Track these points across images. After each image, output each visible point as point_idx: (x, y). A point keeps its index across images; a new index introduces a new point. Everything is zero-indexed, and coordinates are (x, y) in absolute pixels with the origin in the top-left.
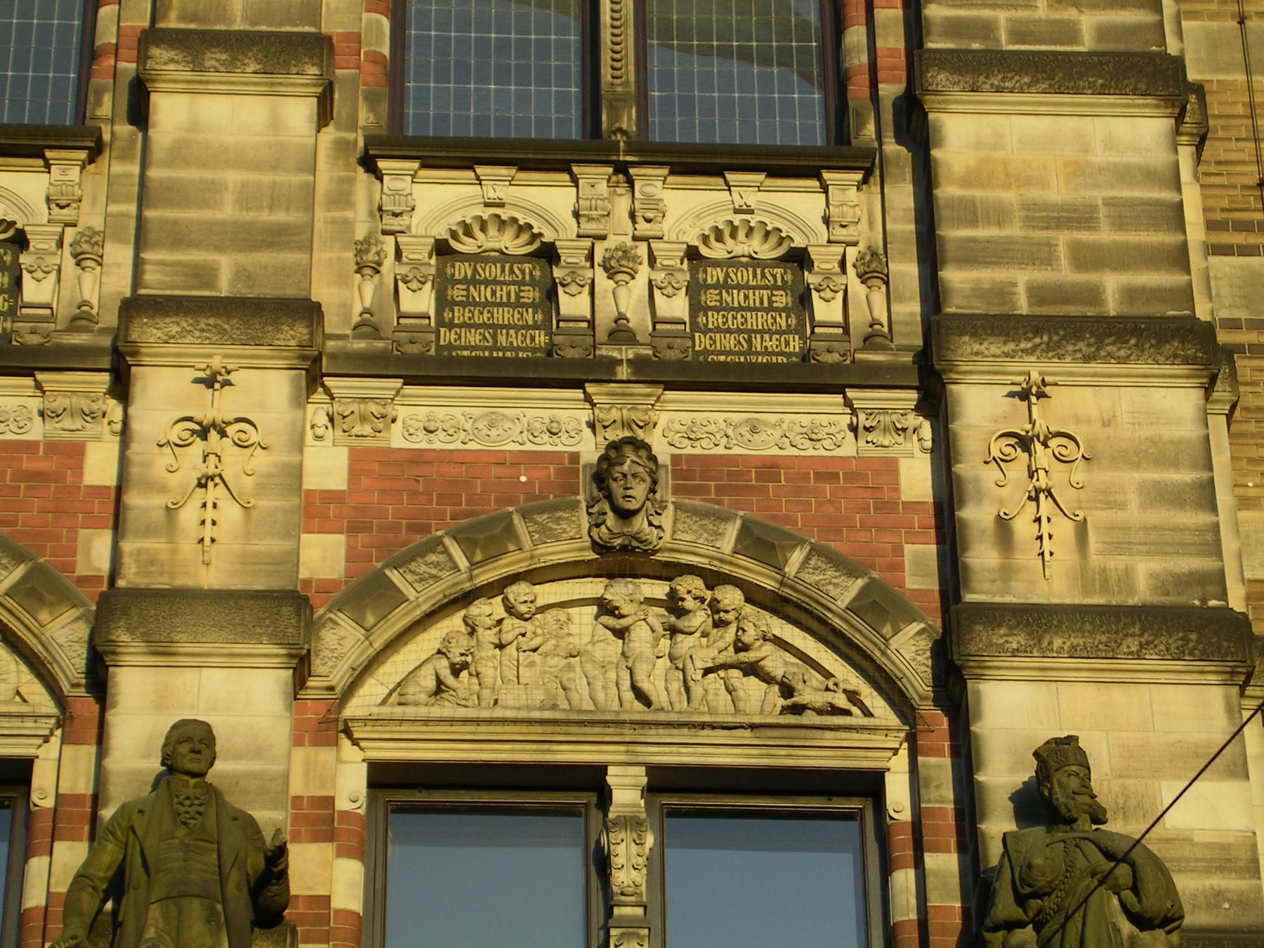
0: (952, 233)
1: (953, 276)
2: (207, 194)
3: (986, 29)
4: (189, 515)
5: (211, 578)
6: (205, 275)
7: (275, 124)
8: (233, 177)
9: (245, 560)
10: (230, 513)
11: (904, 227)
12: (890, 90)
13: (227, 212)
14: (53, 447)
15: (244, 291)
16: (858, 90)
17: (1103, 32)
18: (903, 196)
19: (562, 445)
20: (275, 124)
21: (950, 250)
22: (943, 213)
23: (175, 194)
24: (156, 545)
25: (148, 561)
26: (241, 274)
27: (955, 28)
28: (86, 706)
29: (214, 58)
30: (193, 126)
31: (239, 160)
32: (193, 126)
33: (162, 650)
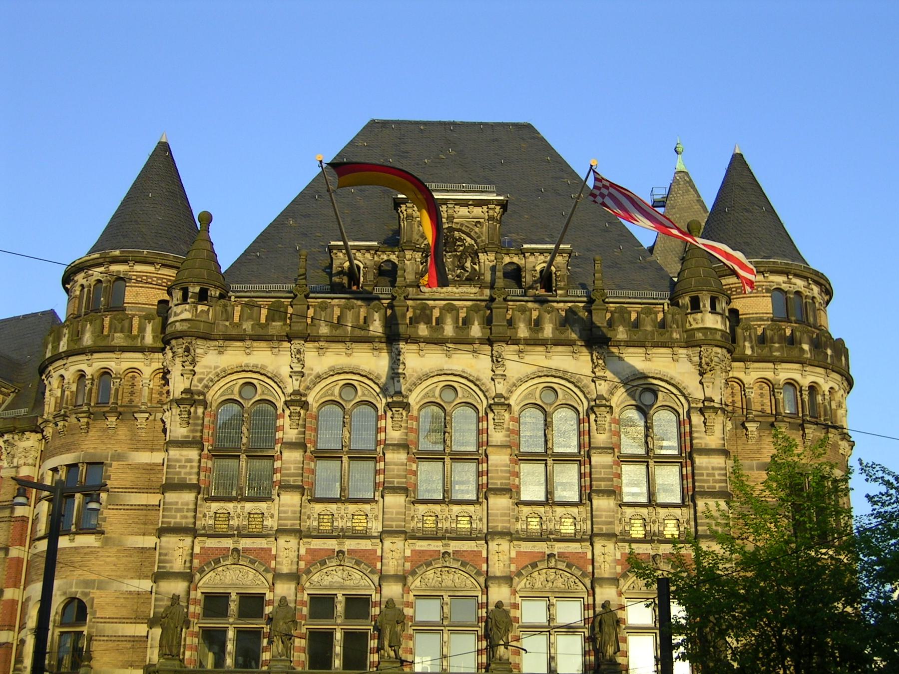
0: (699, 521)
1: (699, 528)
2: (600, 516)
3: (703, 487)
4: (603, 566)
5: (606, 576)
6: (601, 529)
7: (609, 504)
8: (604, 513)
9: (611, 573)
10: (607, 566)
11: (692, 516)
12: (690, 493)
13: (604, 519)
14: (583, 553)
15: (608, 532)
16: (685, 491)
17: (720, 487)
18: (692, 511)
19: (648, 552)
20: (609, 504)
21: (699, 524)
22: (698, 518)
23: (597, 517)
24: (599, 571)
25: (598, 573)
26: (606, 529)
27: (700, 487)
28: (591, 592)
29: (601, 495)
30: (598, 505)
31: (605, 511)
32: (598, 505)
33: (601, 586)
